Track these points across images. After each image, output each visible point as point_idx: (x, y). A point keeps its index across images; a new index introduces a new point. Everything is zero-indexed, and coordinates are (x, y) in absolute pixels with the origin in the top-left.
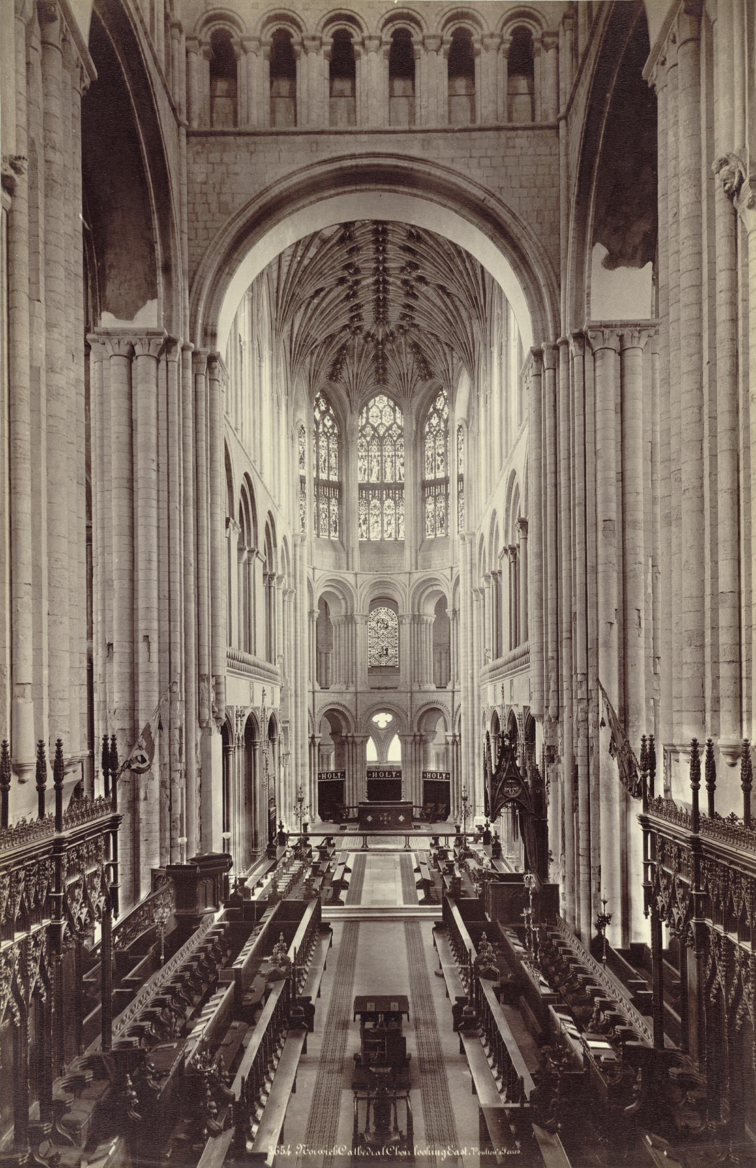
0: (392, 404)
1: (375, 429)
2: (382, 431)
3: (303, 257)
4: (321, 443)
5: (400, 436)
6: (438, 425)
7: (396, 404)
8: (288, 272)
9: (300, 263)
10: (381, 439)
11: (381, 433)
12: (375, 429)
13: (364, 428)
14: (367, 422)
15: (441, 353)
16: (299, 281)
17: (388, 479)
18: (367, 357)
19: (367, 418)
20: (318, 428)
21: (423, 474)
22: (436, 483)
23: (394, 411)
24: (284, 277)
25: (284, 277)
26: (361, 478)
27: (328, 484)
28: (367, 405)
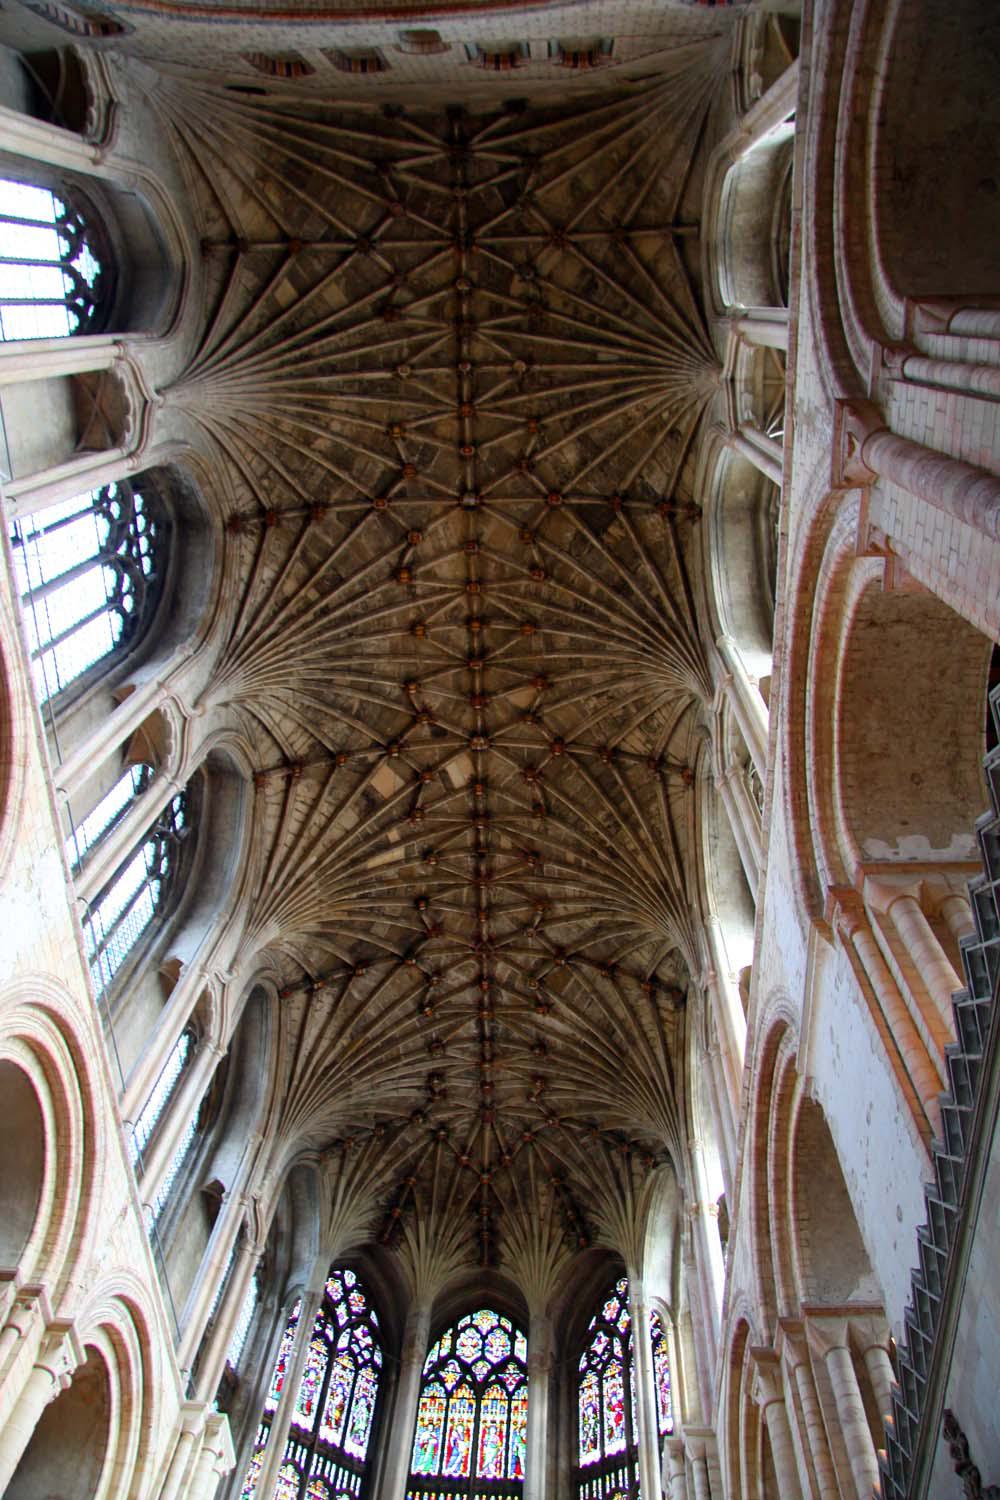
0: (509, 1326)
1: (466, 1368)
2: (481, 1370)
3: (330, 819)
4: (337, 1370)
5: (521, 1383)
6: (609, 1348)
7: (514, 1328)
8: (298, 836)
9: (323, 830)
10: (479, 1389)
11: (479, 1378)
12: (466, 1368)
13: (442, 1363)
14: (452, 1354)
15: (609, 1175)
16: (318, 862)
17: (490, 1471)
18: (457, 1202)
19: (454, 1348)
20: (337, 1336)
21: (574, 1451)
22: (608, 1465)
23: (512, 1338)
24: (287, 839)
25: (287, 839)
26: (425, 1465)
27: (337, 1455)
28: (454, 1326)
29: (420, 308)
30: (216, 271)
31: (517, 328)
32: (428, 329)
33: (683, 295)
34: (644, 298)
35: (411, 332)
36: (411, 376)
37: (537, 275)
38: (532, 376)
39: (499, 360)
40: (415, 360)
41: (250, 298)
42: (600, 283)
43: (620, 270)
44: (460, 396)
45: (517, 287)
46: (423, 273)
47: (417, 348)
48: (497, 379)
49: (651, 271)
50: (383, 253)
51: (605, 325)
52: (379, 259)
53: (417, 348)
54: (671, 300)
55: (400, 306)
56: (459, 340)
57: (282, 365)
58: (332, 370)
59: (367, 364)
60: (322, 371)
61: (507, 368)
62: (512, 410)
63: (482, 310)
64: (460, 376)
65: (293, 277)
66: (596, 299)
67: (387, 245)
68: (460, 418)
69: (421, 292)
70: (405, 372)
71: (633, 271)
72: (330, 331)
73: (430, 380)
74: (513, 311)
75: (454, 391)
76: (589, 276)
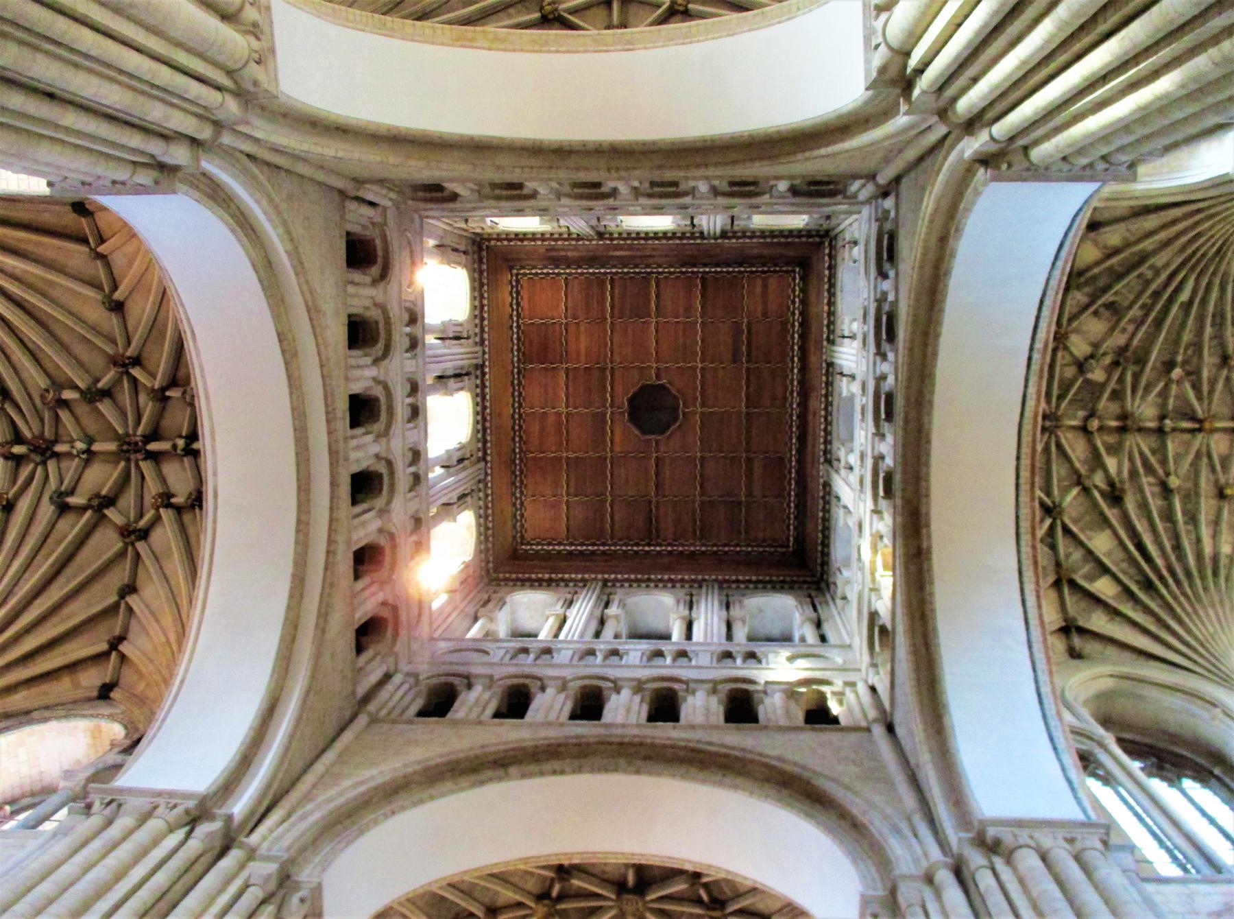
29: (1111, 463)
30: (1090, 647)
31: (1136, 377)
32: (1131, 459)
33: (1151, 222)
34: (1143, 258)
35: (1133, 474)
36: (1177, 475)
37: (1092, 356)
38: (1185, 362)
39: (1164, 394)
40: (1161, 472)
41: (1118, 619)
42: (1111, 299)
43: (1102, 282)
44: (1192, 431)
45: (1097, 375)
46: (1079, 461)
47: (1149, 469)
48: (1182, 397)
49: (1116, 251)
50: (1063, 496)
51: (1157, 295)
52: (1069, 499)
53: (1149, 469)
54: (1150, 234)
55: (1111, 484)
56: (1140, 430)
57: (1185, 594)
58: (1178, 547)
59: (1169, 516)
60: (1181, 557)
61: (1174, 387)
62: (1213, 383)
63: (1114, 408)
64: (1174, 430)
65: (1091, 578)
66: (1126, 303)
67: (1056, 492)
68: (1213, 431)
69: (1096, 461)
70: (1174, 482)
71: (1110, 270)
72: (1141, 547)
73: (1178, 457)
74: (1121, 380)
75: (1187, 436)
76: (1102, 310)
